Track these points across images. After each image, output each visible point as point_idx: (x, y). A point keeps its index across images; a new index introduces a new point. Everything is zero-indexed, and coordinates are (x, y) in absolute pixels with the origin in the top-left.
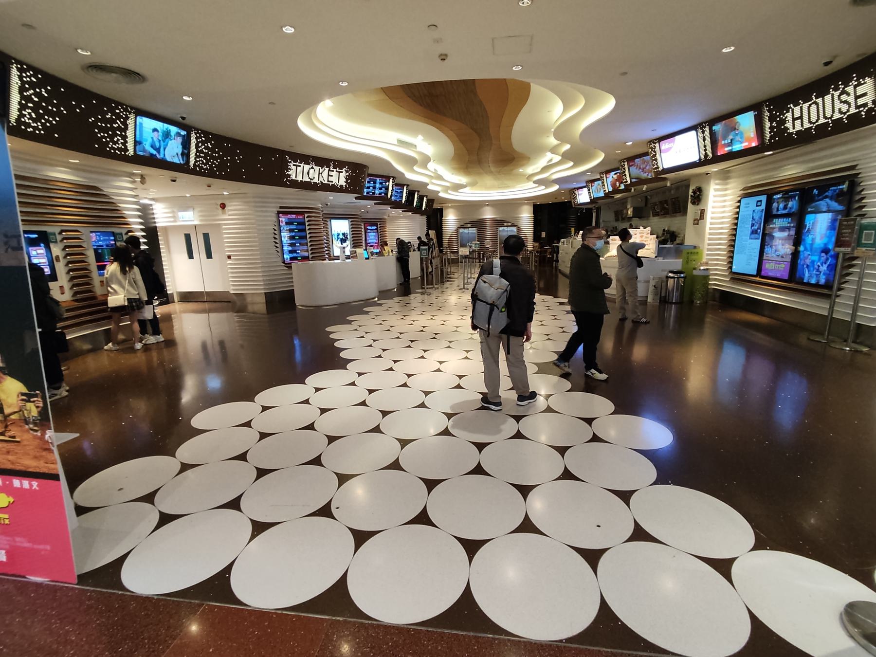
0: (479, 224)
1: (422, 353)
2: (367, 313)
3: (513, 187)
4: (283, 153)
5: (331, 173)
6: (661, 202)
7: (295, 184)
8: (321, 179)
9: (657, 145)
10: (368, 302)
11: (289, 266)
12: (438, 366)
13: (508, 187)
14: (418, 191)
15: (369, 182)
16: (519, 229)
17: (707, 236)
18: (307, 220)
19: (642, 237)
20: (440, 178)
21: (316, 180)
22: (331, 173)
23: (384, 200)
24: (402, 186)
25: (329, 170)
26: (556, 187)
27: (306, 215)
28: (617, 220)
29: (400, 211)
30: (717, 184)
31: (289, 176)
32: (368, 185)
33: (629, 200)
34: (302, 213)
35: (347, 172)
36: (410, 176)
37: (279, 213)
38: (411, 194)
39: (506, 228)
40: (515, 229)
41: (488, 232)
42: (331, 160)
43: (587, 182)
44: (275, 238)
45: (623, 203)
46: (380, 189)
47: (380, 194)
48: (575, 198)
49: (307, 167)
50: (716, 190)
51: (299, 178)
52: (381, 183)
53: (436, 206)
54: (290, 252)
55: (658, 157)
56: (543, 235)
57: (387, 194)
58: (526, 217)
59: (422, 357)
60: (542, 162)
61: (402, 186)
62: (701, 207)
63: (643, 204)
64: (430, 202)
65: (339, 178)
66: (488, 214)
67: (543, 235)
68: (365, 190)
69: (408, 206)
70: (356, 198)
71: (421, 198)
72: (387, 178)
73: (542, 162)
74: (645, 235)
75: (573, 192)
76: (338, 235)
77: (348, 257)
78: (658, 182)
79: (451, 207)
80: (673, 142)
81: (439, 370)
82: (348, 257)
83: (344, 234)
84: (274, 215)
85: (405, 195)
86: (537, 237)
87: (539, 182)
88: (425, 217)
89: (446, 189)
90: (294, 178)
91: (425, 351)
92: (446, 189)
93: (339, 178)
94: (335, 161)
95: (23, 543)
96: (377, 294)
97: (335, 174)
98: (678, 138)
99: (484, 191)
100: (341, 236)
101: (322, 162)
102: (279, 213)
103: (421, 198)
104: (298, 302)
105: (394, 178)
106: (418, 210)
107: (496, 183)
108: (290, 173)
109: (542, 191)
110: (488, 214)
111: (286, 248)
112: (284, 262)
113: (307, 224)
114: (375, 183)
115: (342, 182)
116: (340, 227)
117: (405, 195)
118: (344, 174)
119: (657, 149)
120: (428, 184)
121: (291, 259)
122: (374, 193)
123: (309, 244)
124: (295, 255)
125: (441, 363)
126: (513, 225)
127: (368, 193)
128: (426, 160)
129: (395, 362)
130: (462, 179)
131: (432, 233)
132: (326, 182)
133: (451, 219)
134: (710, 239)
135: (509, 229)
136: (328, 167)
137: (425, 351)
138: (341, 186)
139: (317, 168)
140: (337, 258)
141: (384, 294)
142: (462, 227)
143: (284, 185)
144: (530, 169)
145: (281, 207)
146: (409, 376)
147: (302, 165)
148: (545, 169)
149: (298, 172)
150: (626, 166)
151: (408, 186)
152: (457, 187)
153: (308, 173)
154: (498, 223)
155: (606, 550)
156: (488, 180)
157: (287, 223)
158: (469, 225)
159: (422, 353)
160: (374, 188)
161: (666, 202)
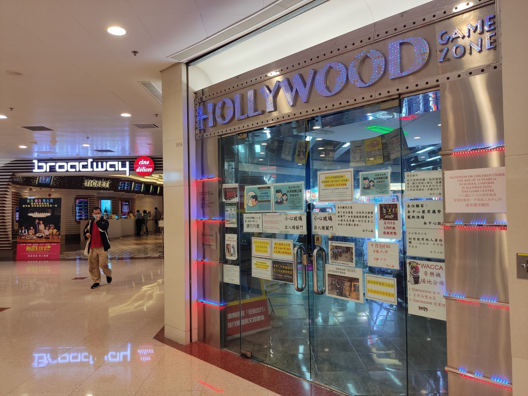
11: (78, 223)
34: (87, 198)
49: (92, 181)
51: (88, 186)
54: (79, 216)
65: (106, 184)
85: (143, 187)
95: (51, 253)
102: (76, 199)
111: (77, 214)
114: (125, 184)
115: (108, 186)
117: (143, 187)
121: (79, 219)
122: (124, 188)
136: (102, 180)
139: (96, 181)
157: (79, 203)
160: (124, 186)
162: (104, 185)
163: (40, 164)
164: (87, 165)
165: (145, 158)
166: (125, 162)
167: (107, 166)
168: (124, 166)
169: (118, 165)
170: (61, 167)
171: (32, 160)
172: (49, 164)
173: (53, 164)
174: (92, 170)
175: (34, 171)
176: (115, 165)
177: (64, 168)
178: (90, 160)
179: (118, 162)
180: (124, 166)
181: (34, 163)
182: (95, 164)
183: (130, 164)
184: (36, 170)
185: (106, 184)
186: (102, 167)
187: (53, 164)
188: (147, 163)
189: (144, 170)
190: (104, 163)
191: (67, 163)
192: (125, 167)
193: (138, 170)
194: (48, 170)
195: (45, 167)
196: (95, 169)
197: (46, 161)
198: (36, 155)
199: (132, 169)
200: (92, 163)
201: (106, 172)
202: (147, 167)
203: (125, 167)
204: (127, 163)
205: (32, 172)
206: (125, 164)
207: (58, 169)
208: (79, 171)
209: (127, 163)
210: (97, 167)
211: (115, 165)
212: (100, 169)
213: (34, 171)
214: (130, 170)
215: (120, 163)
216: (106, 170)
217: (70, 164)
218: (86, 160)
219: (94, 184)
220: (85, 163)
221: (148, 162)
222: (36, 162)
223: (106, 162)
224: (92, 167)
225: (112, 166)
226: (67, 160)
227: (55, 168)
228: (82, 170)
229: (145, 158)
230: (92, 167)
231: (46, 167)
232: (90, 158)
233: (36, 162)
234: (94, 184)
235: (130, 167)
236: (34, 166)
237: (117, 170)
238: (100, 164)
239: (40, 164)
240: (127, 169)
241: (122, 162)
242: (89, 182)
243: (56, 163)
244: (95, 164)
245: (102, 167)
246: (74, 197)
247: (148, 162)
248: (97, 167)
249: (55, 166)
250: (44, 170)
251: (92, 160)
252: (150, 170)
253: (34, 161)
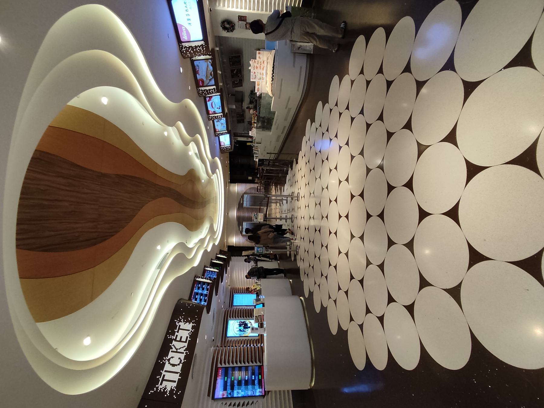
0: (240, 221)
1: (332, 267)
2: (324, 310)
3: (216, 194)
4: (145, 398)
5: (178, 339)
6: (232, 77)
7: (182, 384)
8: (182, 350)
9: (184, 44)
10: (308, 305)
12: (343, 255)
13: (216, 197)
14: (212, 259)
15: (196, 300)
16: (245, 193)
17: (260, 12)
18: (223, 365)
19: (257, 68)
20: (202, 241)
21: (182, 356)
22: (178, 339)
23: (215, 285)
24: (205, 271)
25: (175, 340)
26: (217, 159)
27: (219, 365)
28: (243, 122)
29: (225, 275)
30: (219, 5)
31: (172, 390)
32: (198, 300)
33: (230, 106)
35: (180, 321)
36: (196, 263)
37: (213, 398)
38: (213, 265)
39: (245, 203)
40: (245, 196)
41: (246, 214)
42: (166, 337)
43: (216, 136)
44: (239, 405)
45: (232, 112)
46: (203, 289)
47: (207, 290)
49: (167, 367)
50: (224, 6)
51: (176, 377)
52: (199, 288)
53: (226, 249)
55: (193, 45)
56: (250, 178)
57: (208, 284)
58: (237, 188)
59: (335, 267)
60: (198, 162)
61: (205, 271)
62: (235, 20)
63: (234, 97)
64: (221, 252)
66: (234, 213)
67: (250, 178)
68: (203, 303)
69: (222, 268)
70: (208, 312)
71: (218, 259)
72: (195, 282)
73: (198, 162)
74: (256, 65)
75: (223, 150)
76: (240, 330)
77: (261, 326)
78: (216, 64)
79: (227, 240)
80: (181, 26)
81: (347, 254)
82: (261, 326)
83: (240, 325)
84: (215, 403)
85: (212, 269)
86: (252, 182)
87: (214, 172)
88: (233, 258)
89: (212, 238)
90: (175, 385)
91: (330, 265)
92: (212, 238)
93: (185, 329)
94: (168, 333)
96: (297, 297)
98: (178, 21)
99: (218, 214)
100: (242, 328)
101: (165, 348)
103: (218, 259)
104: (306, 387)
105: (196, 277)
106: (226, 262)
107: (212, 205)
108: (169, 389)
109: (220, 171)
110: (234, 213)
112: (263, 396)
113: (227, 365)
114: (197, 294)
115: (189, 326)
116: (233, 328)
117: (212, 269)
118: (182, 325)
119: (187, 45)
120: (206, 251)
122: (206, 295)
123: (247, 364)
124: (256, 382)
125: (340, 252)
126: (243, 197)
127: (205, 301)
128: (182, 245)
129: (339, 289)
131: (244, 253)
132: (186, 344)
133: (235, 240)
134: (262, 10)
135: (245, 199)
136: (171, 341)
137: (330, 265)
138: (193, 327)
139: (171, 354)
140: (262, 336)
141: (297, 290)
142: (241, 232)
143: (180, 398)
144: (203, 176)
145: (209, 395)
146: (352, 278)
147: (163, 373)
150: (203, 89)
151: (205, 267)
152: (212, 231)
153: (173, 365)
154: (240, 207)
155: (457, 147)
156: (210, 208)
158: (241, 227)
159: (332, 267)
160: (202, 294)
161: (232, 71)
185: (185, 329)
242: (168, 376)
246: (210, 401)
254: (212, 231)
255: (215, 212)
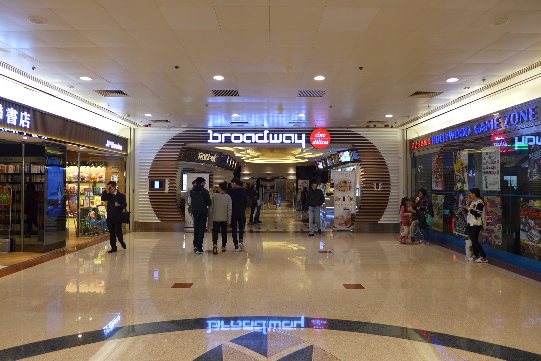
3: (284, 157)
20: (248, 154)
26: (307, 160)
48: (317, 166)
89: (248, 158)
92: (248, 158)
93: (213, 158)
97: (212, 157)
101: (208, 152)
130: (257, 154)
133: (246, 172)
143: (195, 161)
148: (299, 154)
149: (202, 157)
152: (253, 157)
162: (211, 159)
163: (215, 135)
164: (263, 137)
165: (322, 130)
166: (301, 134)
167: (283, 138)
168: (300, 138)
169: (294, 138)
170: (237, 138)
171: (207, 131)
172: (224, 135)
173: (229, 135)
174: (268, 141)
175: (209, 141)
176: (291, 137)
177: (286, 137)
178: (266, 132)
179: (295, 134)
180: (300, 138)
181: (209, 134)
182: (271, 135)
183: (306, 137)
184: (211, 140)
185: (213, 158)
186: (278, 139)
187: (229, 135)
188: (324, 135)
189: (320, 142)
190: (281, 135)
191: (221, 134)
192: (302, 139)
193: (314, 143)
194: (223, 141)
195: (220, 138)
196: (271, 141)
197: (221, 131)
198: (210, 125)
199: (308, 142)
200: (268, 134)
201: (282, 144)
202: (323, 140)
203: (302, 139)
204: (304, 135)
205: (207, 142)
206: (302, 137)
207: (233, 140)
208: (255, 142)
209: (304, 135)
210: (273, 139)
211: (291, 137)
212: (276, 141)
213: (209, 141)
214: (306, 143)
215: (296, 135)
216: (282, 142)
217: (246, 135)
218: (262, 131)
219: (205, 157)
220: (261, 135)
221: (325, 134)
222: (210, 132)
223: (283, 134)
224: (268, 139)
225: (288, 138)
226: (243, 131)
227: (231, 139)
228: (258, 141)
229: (322, 130)
230: (268, 139)
231: (222, 138)
232: (266, 129)
233: (210, 132)
234: (205, 157)
235: (306, 140)
236: (209, 137)
237: (293, 142)
238: (276, 135)
239: (215, 135)
240: (303, 141)
241: (298, 134)
243: (231, 134)
244: (271, 135)
245: (278, 139)
247: (325, 134)
248: (273, 139)
249: (231, 137)
250: (219, 141)
251: (268, 132)
252: (326, 143)
253: (209, 132)
254: (253, 157)
255: (269, 157)
